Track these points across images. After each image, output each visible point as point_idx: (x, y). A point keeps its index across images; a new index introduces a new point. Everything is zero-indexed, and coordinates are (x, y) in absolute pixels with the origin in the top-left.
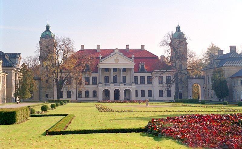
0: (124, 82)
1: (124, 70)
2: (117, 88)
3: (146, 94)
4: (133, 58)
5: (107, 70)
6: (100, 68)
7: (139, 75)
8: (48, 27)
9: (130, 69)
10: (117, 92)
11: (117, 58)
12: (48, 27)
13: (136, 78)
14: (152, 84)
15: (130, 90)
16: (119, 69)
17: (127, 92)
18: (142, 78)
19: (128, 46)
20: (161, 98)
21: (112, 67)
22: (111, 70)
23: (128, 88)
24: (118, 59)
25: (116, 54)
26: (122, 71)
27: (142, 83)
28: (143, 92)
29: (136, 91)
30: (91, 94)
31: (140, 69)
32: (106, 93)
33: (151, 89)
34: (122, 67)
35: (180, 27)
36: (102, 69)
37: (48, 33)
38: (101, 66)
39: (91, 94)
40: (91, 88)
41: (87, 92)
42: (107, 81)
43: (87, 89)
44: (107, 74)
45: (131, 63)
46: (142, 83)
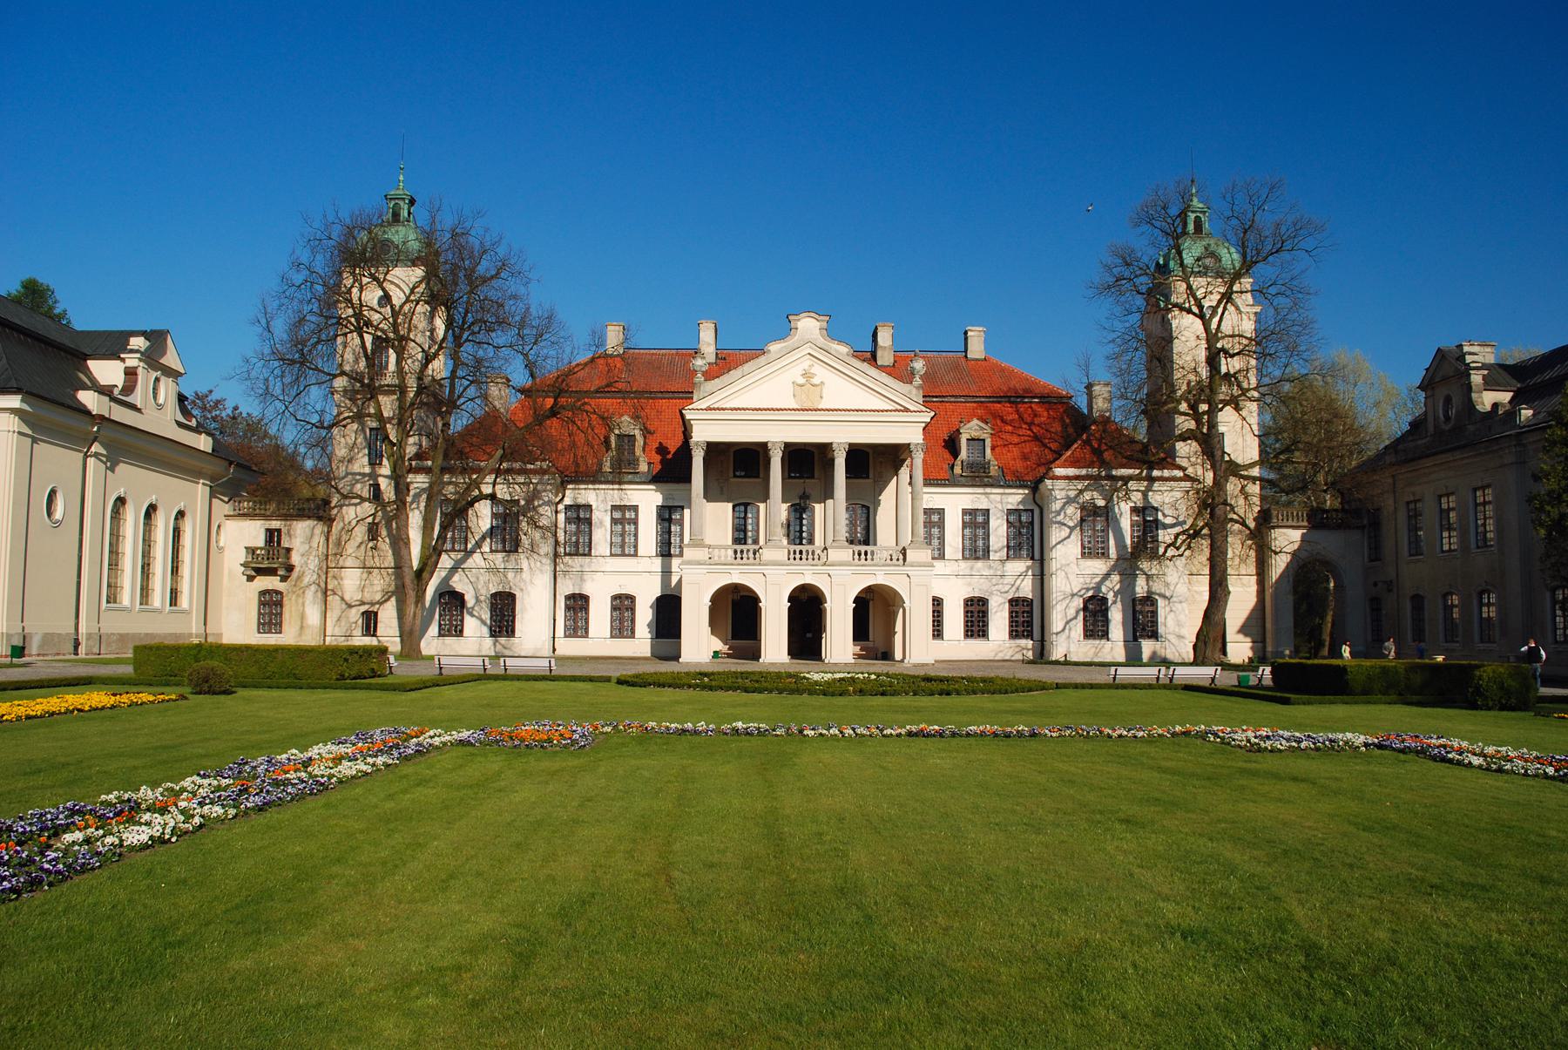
0: (863, 535)
2: (808, 575)
3: (999, 621)
4: (918, 381)
6: (697, 443)
7: (954, 502)
11: (807, 375)
13: (934, 520)
14: (1037, 556)
15: (896, 593)
18: (976, 521)
21: (776, 434)
23: (880, 577)
24: (816, 381)
25: (807, 349)
29: (937, 603)
31: (958, 462)
32: (737, 612)
34: (841, 436)
36: (715, 451)
38: (705, 431)
45: (907, 410)
46: (976, 550)
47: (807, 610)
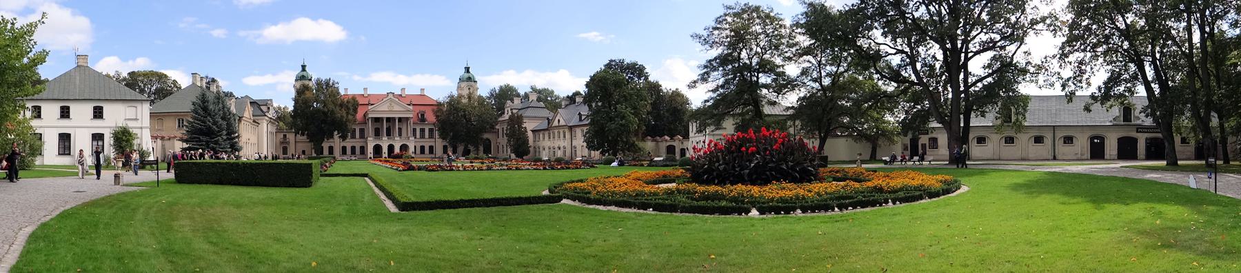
0: (400, 135)
1: (400, 119)
5: (377, 120)
8: (304, 67)
9: (407, 119)
10: (391, 148)
12: (304, 67)
13: (414, 130)
16: (394, 119)
17: (404, 148)
18: (422, 131)
19: (403, 89)
27: (422, 136)
28: (422, 148)
30: (358, 151)
32: (377, 149)
39: (358, 151)
40: (357, 143)
41: (353, 148)
42: (377, 133)
44: (378, 125)
46: (422, 136)
47: (391, 148)
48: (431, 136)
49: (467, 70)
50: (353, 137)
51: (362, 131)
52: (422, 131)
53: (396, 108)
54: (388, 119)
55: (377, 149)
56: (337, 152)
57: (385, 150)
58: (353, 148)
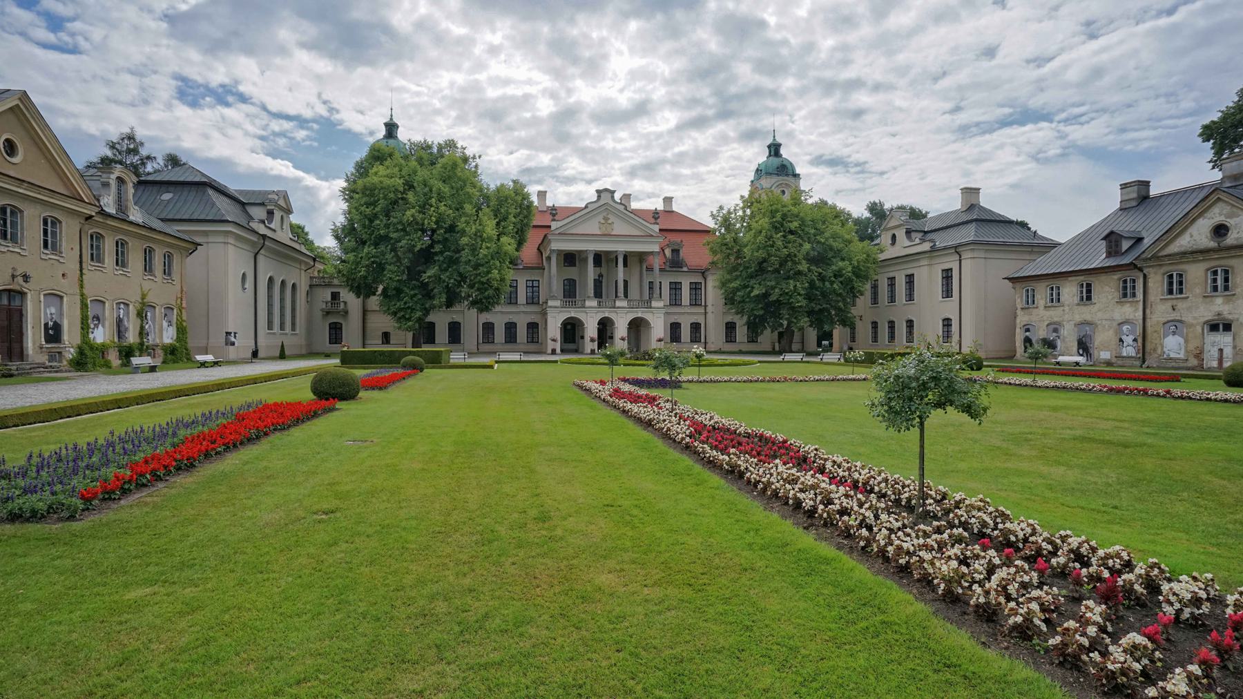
5: (570, 258)
8: (391, 128)
9: (641, 257)
10: (605, 327)
11: (606, 219)
12: (391, 128)
18: (675, 288)
20: (729, 347)
22: (586, 260)
26: (621, 260)
30: (522, 333)
32: (571, 331)
33: (701, 320)
34: (622, 248)
35: (780, 145)
36: (559, 252)
37: (391, 141)
39: (522, 333)
40: (522, 316)
41: (511, 328)
42: (570, 292)
43: (514, 319)
44: (572, 273)
48: (695, 302)
49: (775, 149)
50: (512, 301)
51: (533, 288)
52: (675, 288)
53: (620, 228)
54: (598, 258)
55: (571, 331)
56: (471, 333)
57: (591, 330)
58: (511, 328)
